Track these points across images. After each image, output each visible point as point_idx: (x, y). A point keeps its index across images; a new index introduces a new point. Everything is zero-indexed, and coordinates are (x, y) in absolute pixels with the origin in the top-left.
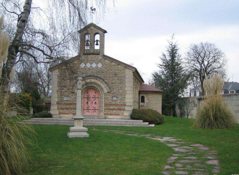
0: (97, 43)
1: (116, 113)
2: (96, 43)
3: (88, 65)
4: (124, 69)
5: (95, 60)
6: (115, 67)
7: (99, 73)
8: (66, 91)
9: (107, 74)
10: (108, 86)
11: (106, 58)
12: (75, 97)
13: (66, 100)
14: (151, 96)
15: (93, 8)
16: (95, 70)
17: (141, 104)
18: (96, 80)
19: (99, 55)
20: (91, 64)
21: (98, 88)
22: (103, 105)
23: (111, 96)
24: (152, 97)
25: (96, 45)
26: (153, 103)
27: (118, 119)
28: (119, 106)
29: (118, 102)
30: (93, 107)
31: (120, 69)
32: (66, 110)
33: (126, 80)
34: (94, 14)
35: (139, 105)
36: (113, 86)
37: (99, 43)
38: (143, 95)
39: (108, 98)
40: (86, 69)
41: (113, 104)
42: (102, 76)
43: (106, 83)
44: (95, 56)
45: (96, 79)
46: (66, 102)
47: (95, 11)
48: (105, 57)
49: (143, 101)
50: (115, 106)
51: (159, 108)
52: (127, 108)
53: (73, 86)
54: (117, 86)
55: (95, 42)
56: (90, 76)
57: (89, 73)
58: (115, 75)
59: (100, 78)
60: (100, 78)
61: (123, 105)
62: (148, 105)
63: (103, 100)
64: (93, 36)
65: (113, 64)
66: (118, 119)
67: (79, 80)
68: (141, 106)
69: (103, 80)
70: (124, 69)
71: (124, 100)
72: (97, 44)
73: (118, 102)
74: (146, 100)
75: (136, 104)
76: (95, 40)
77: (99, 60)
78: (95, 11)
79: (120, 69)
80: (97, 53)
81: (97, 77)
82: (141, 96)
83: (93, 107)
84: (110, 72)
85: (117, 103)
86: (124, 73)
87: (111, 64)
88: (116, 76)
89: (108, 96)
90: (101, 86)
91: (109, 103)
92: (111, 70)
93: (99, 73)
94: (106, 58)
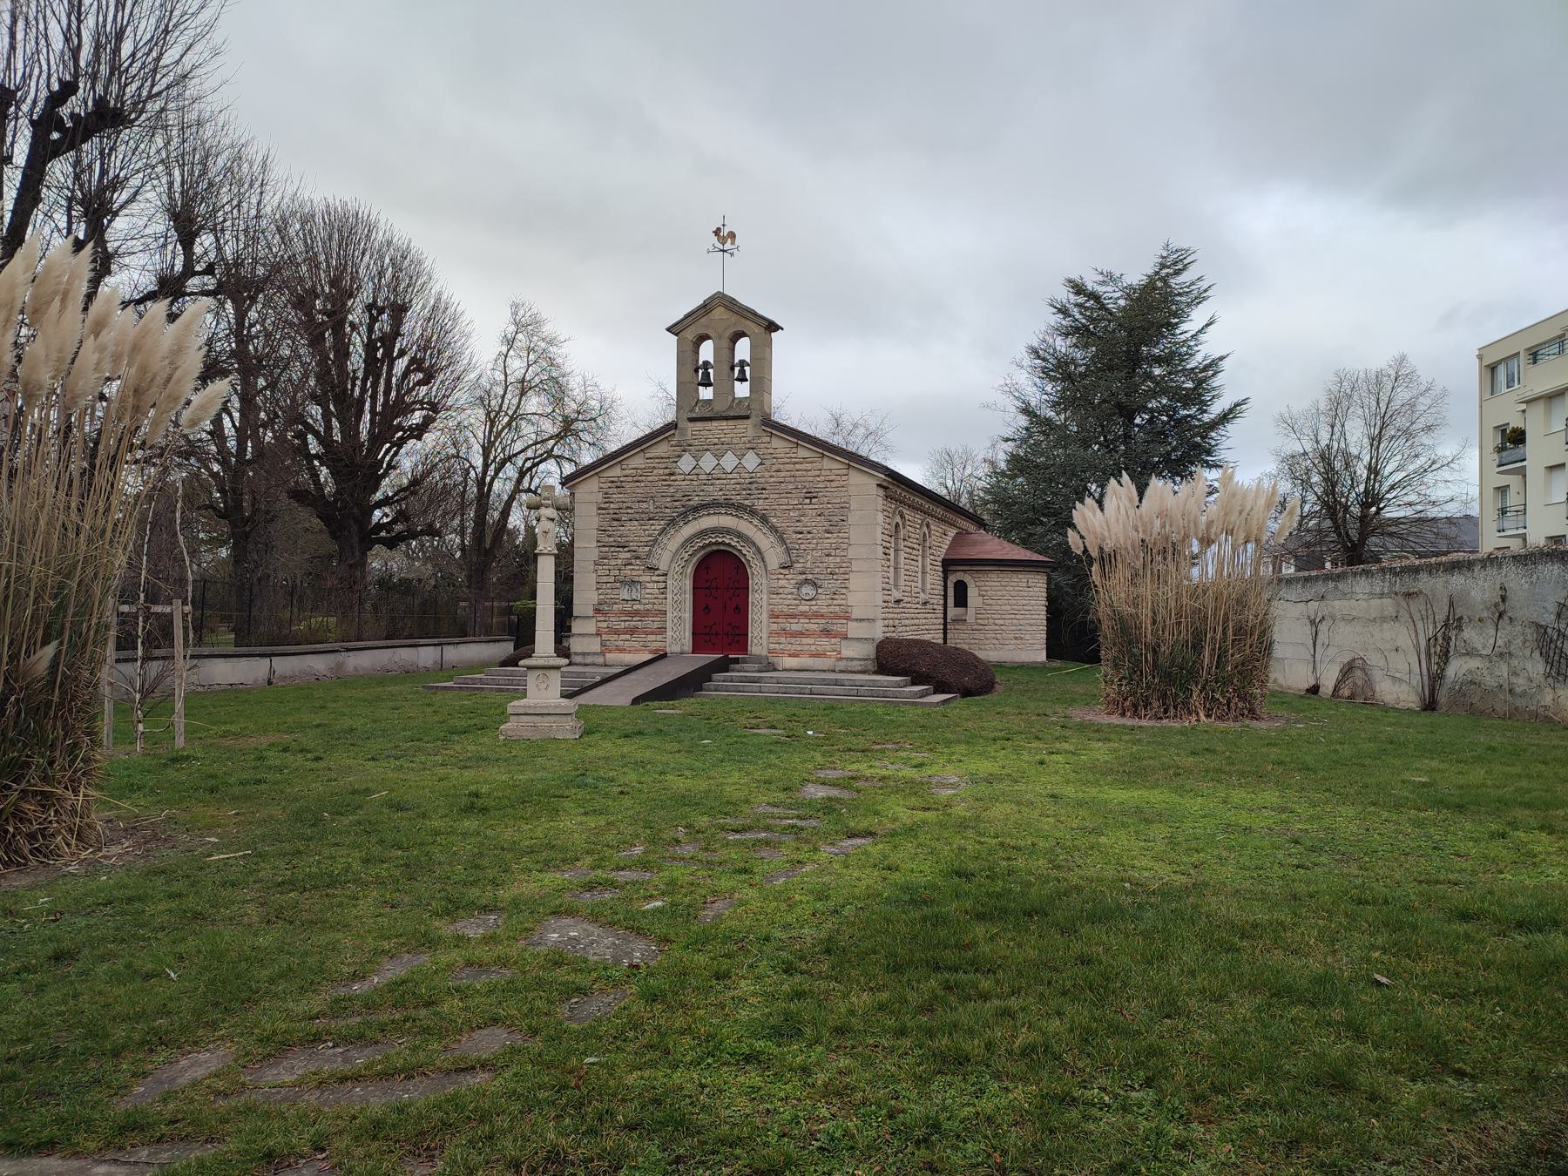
0: (742, 372)
1: (813, 648)
2: (737, 369)
4: (845, 471)
5: (735, 441)
6: (809, 466)
7: (748, 492)
8: (625, 565)
9: (777, 496)
10: (782, 541)
11: (774, 432)
12: (663, 585)
13: (626, 597)
15: (725, 232)
16: (732, 482)
17: (953, 612)
19: (745, 421)
20: (718, 457)
21: (745, 552)
22: (765, 615)
23: (792, 582)
24: (998, 584)
25: (738, 380)
26: (1003, 608)
27: (824, 671)
28: (824, 621)
29: (822, 605)
30: (730, 624)
31: (828, 473)
32: (628, 637)
33: (853, 518)
34: (732, 254)
35: (945, 618)
36: (800, 542)
37: (747, 369)
38: (959, 576)
39: (781, 590)
40: (701, 477)
41: (804, 615)
42: (760, 505)
43: (774, 529)
44: (731, 423)
45: (738, 517)
46: (628, 607)
47: (733, 243)
48: (769, 430)
49: (961, 601)
50: (807, 621)
51: (1029, 628)
52: (854, 629)
53: (653, 546)
54: (815, 541)
55: (732, 369)
56: (715, 504)
57: (714, 493)
59: (753, 513)
60: (753, 513)
62: (981, 616)
63: (765, 597)
64: (725, 343)
65: (802, 453)
66: (824, 671)
67: (543, 519)
68: (953, 620)
69: (764, 519)
70: (845, 471)
71: (844, 597)
72: (742, 379)
73: (819, 603)
74: (972, 593)
75: (916, 611)
76: (736, 361)
78: (733, 243)
79: (828, 473)
81: (740, 508)
82: (952, 579)
83: (730, 624)
85: (815, 608)
86: (844, 489)
87: (793, 456)
88: (814, 500)
89: (782, 583)
90: (754, 544)
91: (785, 609)
93: (748, 492)
94: (774, 432)
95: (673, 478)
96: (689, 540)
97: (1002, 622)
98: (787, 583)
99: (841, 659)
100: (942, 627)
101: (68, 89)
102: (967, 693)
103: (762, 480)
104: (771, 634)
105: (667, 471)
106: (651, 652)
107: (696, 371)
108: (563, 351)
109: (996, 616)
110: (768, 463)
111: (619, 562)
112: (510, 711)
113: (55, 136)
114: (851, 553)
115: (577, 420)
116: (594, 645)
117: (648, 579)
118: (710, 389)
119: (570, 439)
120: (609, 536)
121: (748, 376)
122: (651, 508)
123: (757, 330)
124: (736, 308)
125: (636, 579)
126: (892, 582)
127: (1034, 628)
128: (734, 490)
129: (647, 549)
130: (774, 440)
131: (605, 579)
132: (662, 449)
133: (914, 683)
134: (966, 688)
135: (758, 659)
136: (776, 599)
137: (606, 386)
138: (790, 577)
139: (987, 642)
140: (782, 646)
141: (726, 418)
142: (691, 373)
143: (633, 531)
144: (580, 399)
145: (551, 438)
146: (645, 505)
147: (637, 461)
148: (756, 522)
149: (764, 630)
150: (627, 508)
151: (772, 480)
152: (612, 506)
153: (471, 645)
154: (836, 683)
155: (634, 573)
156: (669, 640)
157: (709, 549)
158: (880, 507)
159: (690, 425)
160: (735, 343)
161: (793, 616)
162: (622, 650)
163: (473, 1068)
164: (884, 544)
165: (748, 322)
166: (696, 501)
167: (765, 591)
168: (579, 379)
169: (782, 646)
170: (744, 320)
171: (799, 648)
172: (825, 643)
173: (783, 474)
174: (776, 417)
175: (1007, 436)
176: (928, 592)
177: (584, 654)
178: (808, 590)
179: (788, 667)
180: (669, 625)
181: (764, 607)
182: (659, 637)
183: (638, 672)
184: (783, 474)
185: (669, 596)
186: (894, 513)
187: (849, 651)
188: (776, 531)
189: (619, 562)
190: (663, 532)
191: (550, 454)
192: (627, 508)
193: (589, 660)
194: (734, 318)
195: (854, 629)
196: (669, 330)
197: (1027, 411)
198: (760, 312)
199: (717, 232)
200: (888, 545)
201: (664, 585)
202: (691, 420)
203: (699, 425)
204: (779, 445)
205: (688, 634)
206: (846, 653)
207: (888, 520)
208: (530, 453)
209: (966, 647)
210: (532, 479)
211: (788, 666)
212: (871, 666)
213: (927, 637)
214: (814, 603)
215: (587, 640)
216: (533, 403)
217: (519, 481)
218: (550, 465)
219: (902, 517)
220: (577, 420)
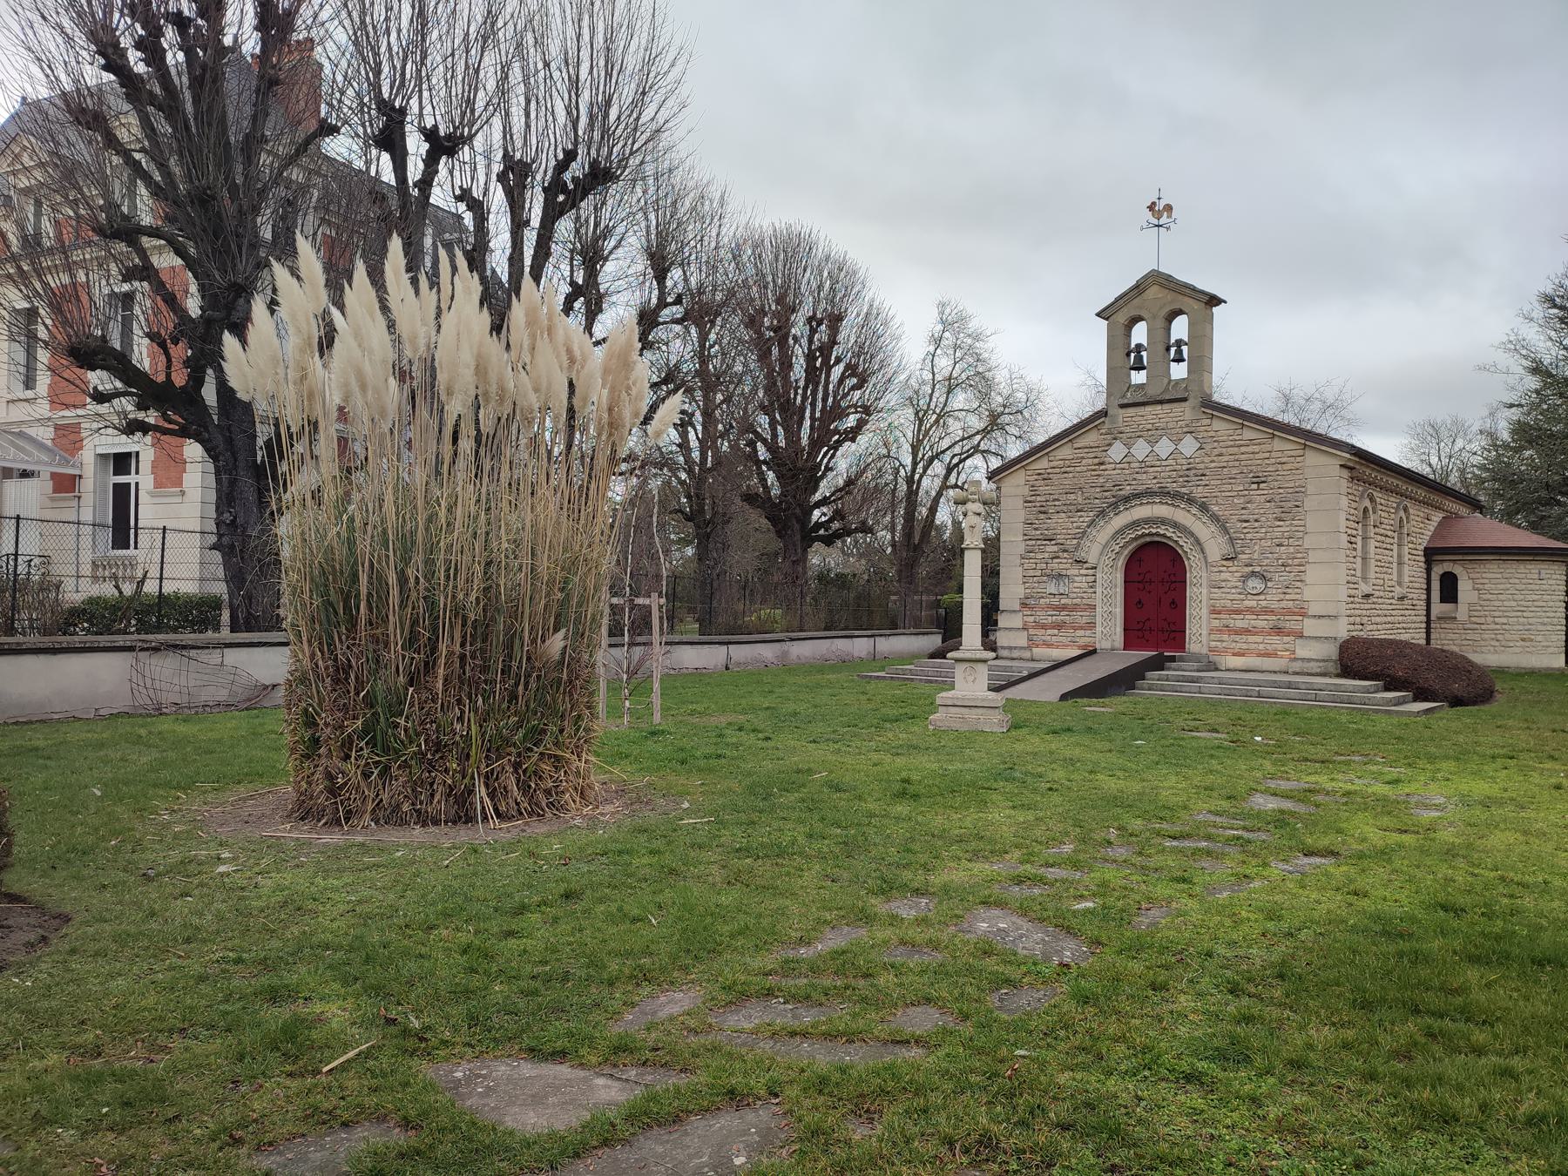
0: (1179, 352)
1: (1261, 647)
2: (1173, 350)
3: (1141, 449)
6: (1256, 449)
10: (1226, 531)
12: (1092, 578)
14: (1492, 573)
17: (1438, 608)
18: (1171, 508)
19: (1183, 404)
20: (1152, 443)
22: (1205, 611)
25: (1174, 361)
29: (1272, 600)
31: (1280, 454)
33: (1309, 503)
34: (1168, 229)
37: (1185, 349)
38: (1447, 567)
39: (1223, 584)
40: (1132, 465)
41: (1251, 610)
42: (1198, 493)
43: (1215, 518)
44: (1166, 406)
46: (1055, 601)
47: (1169, 216)
49: (1449, 591)
51: (1540, 628)
52: (1310, 627)
54: (1263, 530)
55: (1168, 349)
56: (1149, 493)
57: (1147, 481)
58: (1258, 483)
59: (1191, 501)
60: (1191, 501)
61: (1295, 614)
63: (1205, 591)
64: (1160, 323)
65: (1248, 434)
67: (970, 513)
68: (1439, 618)
69: (1204, 508)
72: (1179, 360)
73: (1269, 597)
74: (1464, 587)
76: (1173, 341)
77: (1187, 426)
78: (1169, 216)
79: (1280, 454)
80: (1174, 397)
81: (1176, 496)
82: (1438, 571)
84: (1235, 471)
85: (1264, 603)
88: (1262, 486)
90: (1192, 534)
91: (1229, 604)
92: (1237, 463)
95: (1102, 467)
96: (1120, 532)
97: (1504, 620)
98: (1232, 575)
99: (1296, 659)
100: (1424, 625)
101: (570, 156)
102: (1456, 702)
103: (1202, 466)
104: (1211, 631)
105: (1096, 461)
106: (1080, 647)
107: (1128, 355)
108: (990, 345)
109: (1496, 614)
110: (1208, 447)
111: (1046, 555)
112: (938, 702)
113: (561, 198)
114: (1308, 542)
115: (1003, 413)
116: (1021, 640)
117: (1076, 572)
118: (1144, 373)
119: (995, 434)
120: (1036, 529)
121: (1185, 355)
122: (1080, 499)
123: (1196, 306)
124: (1172, 285)
125: (1064, 572)
126: (1359, 573)
127: (1549, 628)
128: (1170, 477)
129: (1075, 542)
130: (1215, 422)
131: (1031, 573)
132: (1091, 438)
133: (1387, 689)
134: (1456, 697)
135: (1197, 658)
136: (1217, 593)
137: (1032, 377)
138: (1234, 569)
139: (1483, 643)
140: (1224, 644)
141: (1161, 402)
142: (1123, 357)
143: (1060, 524)
144: (1006, 392)
145: (977, 433)
146: (1073, 497)
147: (1065, 452)
148: (1194, 510)
149: (1204, 627)
150: (1055, 500)
151: (1213, 465)
152: (1039, 498)
153: (902, 637)
154: (1289, 686)
155: (1061, 566)
156: (1098, 635)
157: (1142, 541)
158: (1344, 491)
159: (1123, 411)
160: (1170, 322)
161: (1238, 612)
162: (1049, 645)
163: (908, 1042)
164: (1350, 532)
165: (1186, 299)
166: (1127, 490)
167: (1204, 584)
168: (1005, 373)
169: (1224, 644)
170: (1181, 297)
171: (1245, 646)
172: (1276, 642)
173: (1226, 458)
174: (1216, 398)
175: (1512, 401)
176: (1406, 585)
177: (1010, 648)
178: (1255, 584)
179: (1231, 667)
180: (1099, 620)
181: (1204, 603)
182: (1088, 633)
183: (1066, 667)
184: (1226, 458)
185: (1099, 590)
186: (1361, 497)
187: (1305, 650)
188: (1218, 520)
189: (1046, 555)
190: (1092, 523)
191: (976, 449)
192: (1055, 500)
193: (1016, 654)
194: (1170, 296)
195: (1310, 627)
196: (1098, 315)
197: (1537, 369)
198: (1200, 286)
199: (1151, 207)
200: (1354, 532)
201: (1092, 578)
202: (1123, 406)
203: (1131, 411)
204: (1221, 426)
205: (1119, 630)
206: (1300, 653)
207: (1354, 505)
208: (957, 449)
209: (1455, 649)
210: (959, 474)
211: (1231, 666)
212: (1331, 667)
213: (1405, 637)
214: (1262, 597)
215: (1012, 634)
216: (960, 400)
217: (947, 477)
218: (977, 460)
219: (1372, 500)
220: (1003, 413)
